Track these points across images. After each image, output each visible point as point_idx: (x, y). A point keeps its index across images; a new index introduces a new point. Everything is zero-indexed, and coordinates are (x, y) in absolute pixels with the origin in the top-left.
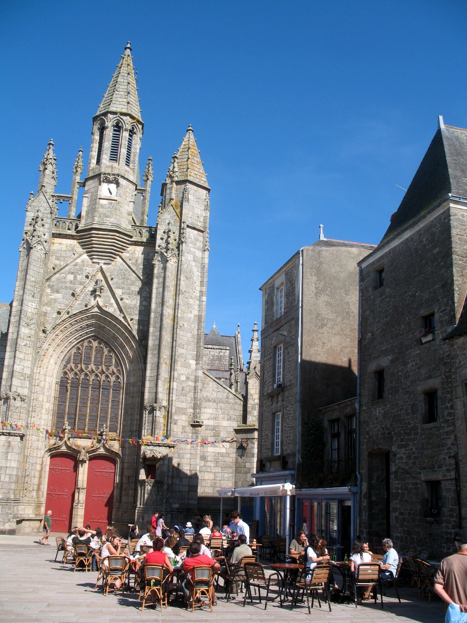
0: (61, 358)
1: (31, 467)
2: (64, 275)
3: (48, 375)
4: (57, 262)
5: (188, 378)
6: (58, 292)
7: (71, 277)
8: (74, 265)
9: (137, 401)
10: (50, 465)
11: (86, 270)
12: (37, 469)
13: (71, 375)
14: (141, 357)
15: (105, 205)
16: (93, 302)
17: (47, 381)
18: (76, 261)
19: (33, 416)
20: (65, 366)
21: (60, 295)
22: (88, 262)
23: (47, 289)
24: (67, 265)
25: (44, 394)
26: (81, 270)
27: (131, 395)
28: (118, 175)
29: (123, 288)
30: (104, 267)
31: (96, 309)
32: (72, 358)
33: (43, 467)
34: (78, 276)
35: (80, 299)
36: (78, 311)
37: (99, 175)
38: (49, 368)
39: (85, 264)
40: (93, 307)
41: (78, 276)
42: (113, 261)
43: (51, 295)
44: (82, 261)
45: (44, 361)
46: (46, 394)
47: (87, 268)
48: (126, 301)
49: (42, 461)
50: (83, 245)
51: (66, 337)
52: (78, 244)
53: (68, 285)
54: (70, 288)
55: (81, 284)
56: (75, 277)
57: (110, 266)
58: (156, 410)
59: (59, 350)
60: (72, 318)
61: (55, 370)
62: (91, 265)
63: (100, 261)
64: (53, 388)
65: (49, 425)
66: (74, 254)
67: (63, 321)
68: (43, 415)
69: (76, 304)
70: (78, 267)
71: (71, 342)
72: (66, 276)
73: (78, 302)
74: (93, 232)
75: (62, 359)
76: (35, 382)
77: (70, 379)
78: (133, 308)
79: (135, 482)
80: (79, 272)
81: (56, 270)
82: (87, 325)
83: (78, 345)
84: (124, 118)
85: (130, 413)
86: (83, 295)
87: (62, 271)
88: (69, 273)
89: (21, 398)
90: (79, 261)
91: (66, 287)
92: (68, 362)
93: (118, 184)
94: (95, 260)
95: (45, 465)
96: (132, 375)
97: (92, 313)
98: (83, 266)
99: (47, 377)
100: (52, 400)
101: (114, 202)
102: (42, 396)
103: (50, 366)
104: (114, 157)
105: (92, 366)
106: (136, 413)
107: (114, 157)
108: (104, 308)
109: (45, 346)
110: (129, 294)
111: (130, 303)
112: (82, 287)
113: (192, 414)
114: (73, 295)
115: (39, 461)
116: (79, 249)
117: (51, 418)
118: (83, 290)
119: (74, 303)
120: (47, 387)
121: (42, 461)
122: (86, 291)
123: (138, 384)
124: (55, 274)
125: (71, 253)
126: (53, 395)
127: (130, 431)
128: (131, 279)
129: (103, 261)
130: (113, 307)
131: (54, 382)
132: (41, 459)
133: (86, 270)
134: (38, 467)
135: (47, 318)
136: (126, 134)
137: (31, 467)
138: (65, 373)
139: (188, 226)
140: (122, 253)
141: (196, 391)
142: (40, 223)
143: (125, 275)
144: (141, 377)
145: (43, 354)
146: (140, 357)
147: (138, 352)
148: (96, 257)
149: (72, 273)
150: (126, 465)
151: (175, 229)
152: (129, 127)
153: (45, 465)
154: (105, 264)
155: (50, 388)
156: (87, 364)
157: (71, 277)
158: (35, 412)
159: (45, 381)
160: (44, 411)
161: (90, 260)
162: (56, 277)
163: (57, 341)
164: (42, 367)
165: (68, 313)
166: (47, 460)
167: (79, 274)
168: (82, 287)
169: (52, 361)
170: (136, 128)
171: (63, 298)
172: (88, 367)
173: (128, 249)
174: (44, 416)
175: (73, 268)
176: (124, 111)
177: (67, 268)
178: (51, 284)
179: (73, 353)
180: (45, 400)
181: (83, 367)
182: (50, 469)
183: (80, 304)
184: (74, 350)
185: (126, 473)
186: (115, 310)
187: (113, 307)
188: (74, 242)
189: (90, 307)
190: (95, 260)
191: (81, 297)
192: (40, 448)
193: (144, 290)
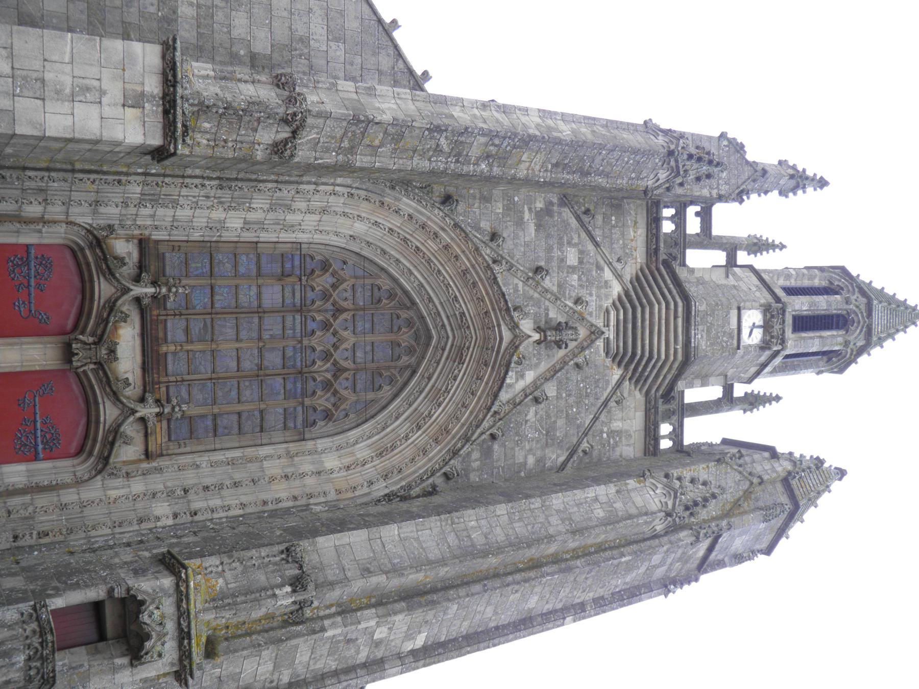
0: (366, 252)
1: (32, 184)
2: (576, 240)
3: (325, 217)
4: (599, 218)
5: (378, 644)
6: (539, 227)
7: (572, 258)
8: (597, 263)
9: (283, 495)
10: (39, 246)
11: (591, 295)
12: (24, 207)
14: (403, 483)
15: (729, 324)
16: (526, 326)
17: (308, 217)
18: (606, 269)
19: (207, 183)
21: (533, 235)
22: (607, 296)
23: (542, 199)
24: (597, 245)
25: (271, 209)
26: (590, 283)
27: (291, 470)
29: (558, 397)
30: (600, 343)
32: (368, 281)
33: (32, 226)
34: (575, 277)
35: (527, 288)
36: (504, 289)
38: (342, 220)
39: (603, 291)
40: (514, 326)
41: (575, 277)
42: (613, 360)
43: (530, 209)
44: (606, 282)
45: (365, 205)
46: (271, 216)
47: (594, 298)
48: (533, 410)
49: (55, 222)
51: (429, 261)
52: (639, 267)
53: (556, 253)
54: (549, 260)
55: (560, 286)
56: (573, 269)
57: (603, 354)
58: (294, 591)
59: (391, 245)
60: (485, 273)
61: (335, 238)
62: (601, 307)
63: (611, 328)
64: (285, 236)
65: (175, 232)
66: (619, 260)
67: (477, 249)
68: (206, 213)
69: (516, 281)
70: (594, 273)
71: (411, 273)
72: (575, 245)
73: (520, 284)
74: (680, 304)
75: (364, 253)
76: (309, 183)
77: (310, 283)
78: (517, 434)
79: (18, 548)
80: (584, 279)
81: (586, 219)
82: (463, 314)
83: (399, 292)
85: (237, 476)
86: (536, 295)
87: (583, 235)
88: (581, 252)
89: (285, 142)
90: (608, 274)
91: (549, 249)
94: (613, 314)
95: (40, 231)
96: (347, 461)
97: (499, 325)
98: (599, 288)
99: (317, 217)
100: (248, 236)
101: (735, 342)
102: (266, 207)
103: (348, 222)
106: (244, 499)
108: (515, 358)
109: (408, 204)
110: (548, 416)
111: (529, 424)
112: (555, 289)
113: (274, 684)
114: (538, 270)
115: (56, 211)
116: (630, 271)
117: (196, 236)
118: (549, 296)
119: (519, 274)
120: (291, 218)
121: (55, 222)
122: (547, 303)
123: (328, 487)
124: (578, 218)
125: (620, 253)
126: (264, 236)
127: (186, 491)
128: (579, 413)
129: (612, 337)
130: (517, 380)
131: (302, 237)
132: (63, 217)
133: (591, 295)
134: (33, 210)
135: (476, 205)
137: (32, 184)
138: (325, 266)
140: (630, 379)
141: (343, 677)
143: (587, 395)
144: (350, 495)
145: (387, 200)
146: (401, 479)
147: (414, 472)
148: (621, 317)
149: (581, 262)
150: (69, 496)
153: (40, 231)
154: (607, 342)
155: (290, 227)
157: (572, 258)
158: (221, 187)
159: (309, 211)
160: (218, 214)
161: (611, 301)
162: (570, 221)
163: (418, 238)
164: (349, 201)
165: (495, 262)
166: (55, 235)
167: (580, 279)
168: (555, 289)
169: (360, 228)
170: (839, 360)
171: (527, 245)
172: (346, 329)
173: (637, 393)
174: (201, 220)
175: (591, 261)
177: (590, 247)
178: (555, 208)
179: (379, 282)
180: (252, 216)
182: (27, 246)
183: (516, 290)
185: (42, 500)
186: (510, 386)
187: (517, 380)
188: (640, 257)
189: (516, 319)
190: (613, 314)
191: (531, 292)
192: (102, 210)
193: (559, 452)
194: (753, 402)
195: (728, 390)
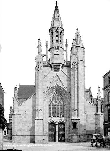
13: (52, 103)
20: (50, 101)
28: (59, 47)
31: (57, 86)
37: (54, 47)
50: (51, 68)
84: (58, 28)
92: (51, 100)
93: (59, 49)
104: (57, 41)
105: (57, 101)
107: (57, 41)
136: (59, 33)
138: (50, 103)
139: (80, 60)
142: (40, 63)
151: (76, 61)
152: (60, 31)
156: (55, 100)
176: (58, 26)
181: (55, 101)
184: (52, 97)
188: (49, 68)
194: (66, 46)
195: (64, 51)
